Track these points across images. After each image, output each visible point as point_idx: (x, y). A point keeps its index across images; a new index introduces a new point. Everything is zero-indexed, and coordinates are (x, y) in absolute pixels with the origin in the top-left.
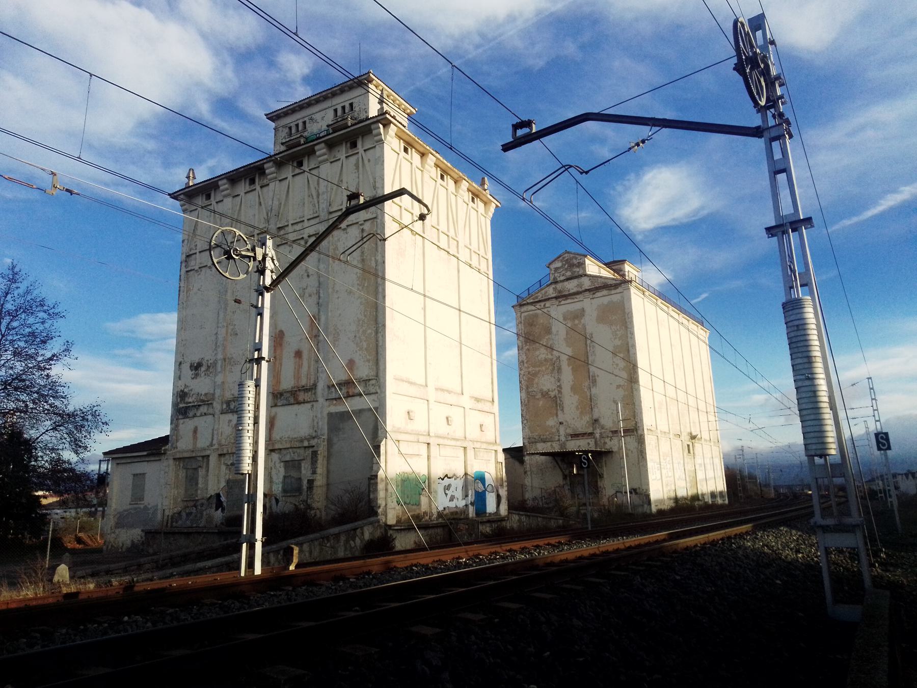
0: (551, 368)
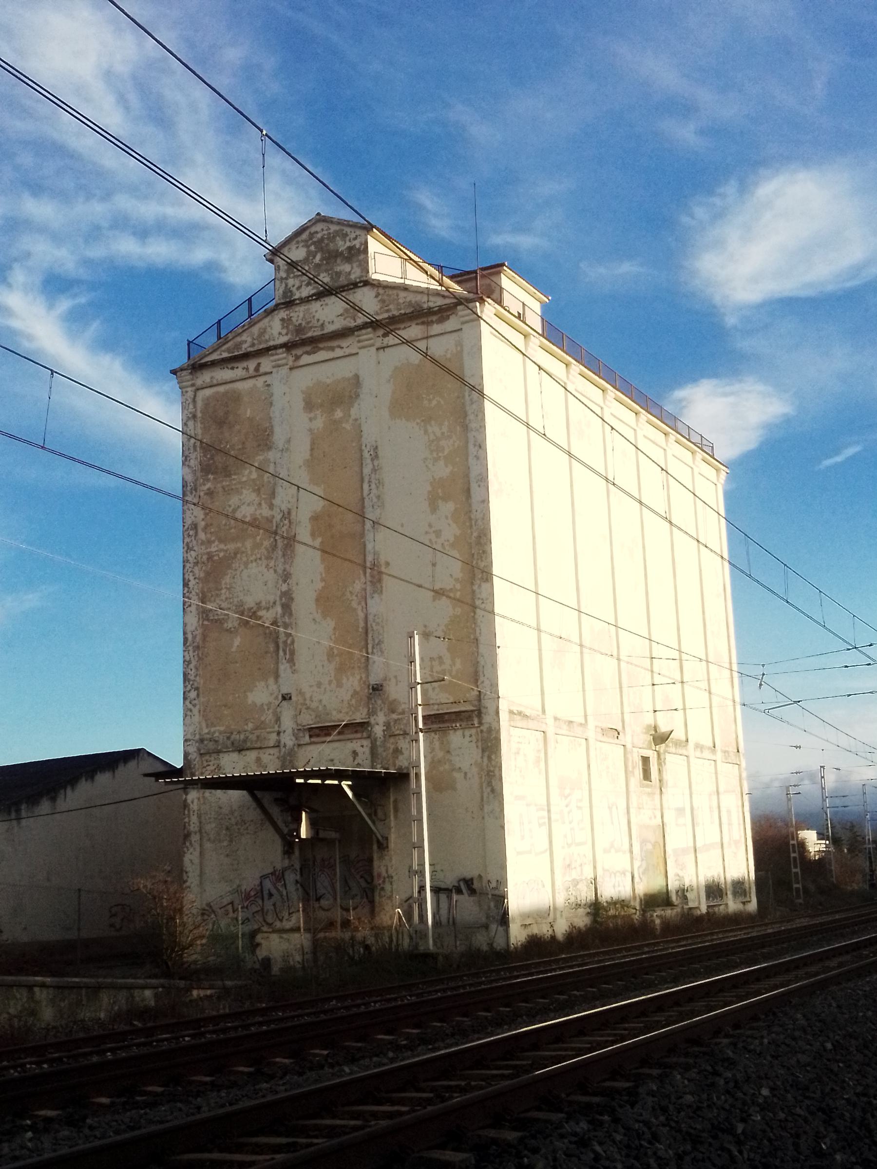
0: (266, 543)
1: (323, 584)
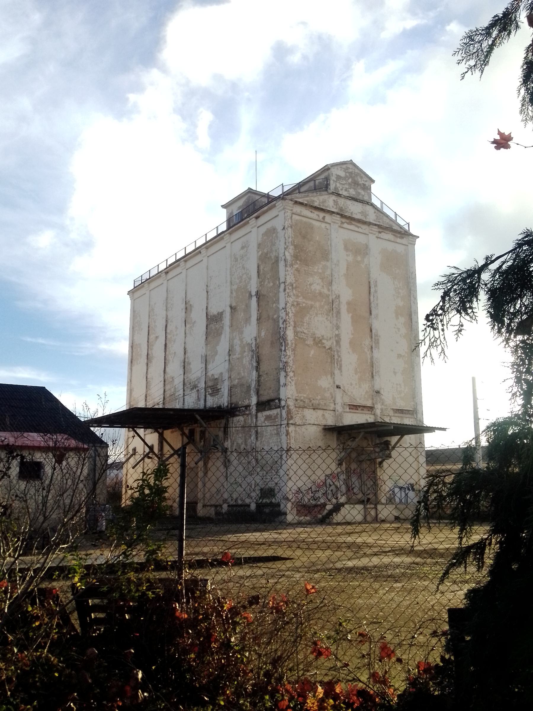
1: (352, 336)
